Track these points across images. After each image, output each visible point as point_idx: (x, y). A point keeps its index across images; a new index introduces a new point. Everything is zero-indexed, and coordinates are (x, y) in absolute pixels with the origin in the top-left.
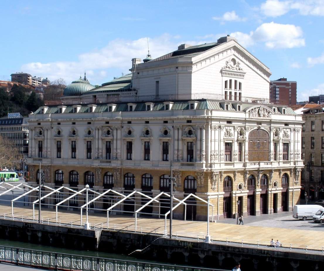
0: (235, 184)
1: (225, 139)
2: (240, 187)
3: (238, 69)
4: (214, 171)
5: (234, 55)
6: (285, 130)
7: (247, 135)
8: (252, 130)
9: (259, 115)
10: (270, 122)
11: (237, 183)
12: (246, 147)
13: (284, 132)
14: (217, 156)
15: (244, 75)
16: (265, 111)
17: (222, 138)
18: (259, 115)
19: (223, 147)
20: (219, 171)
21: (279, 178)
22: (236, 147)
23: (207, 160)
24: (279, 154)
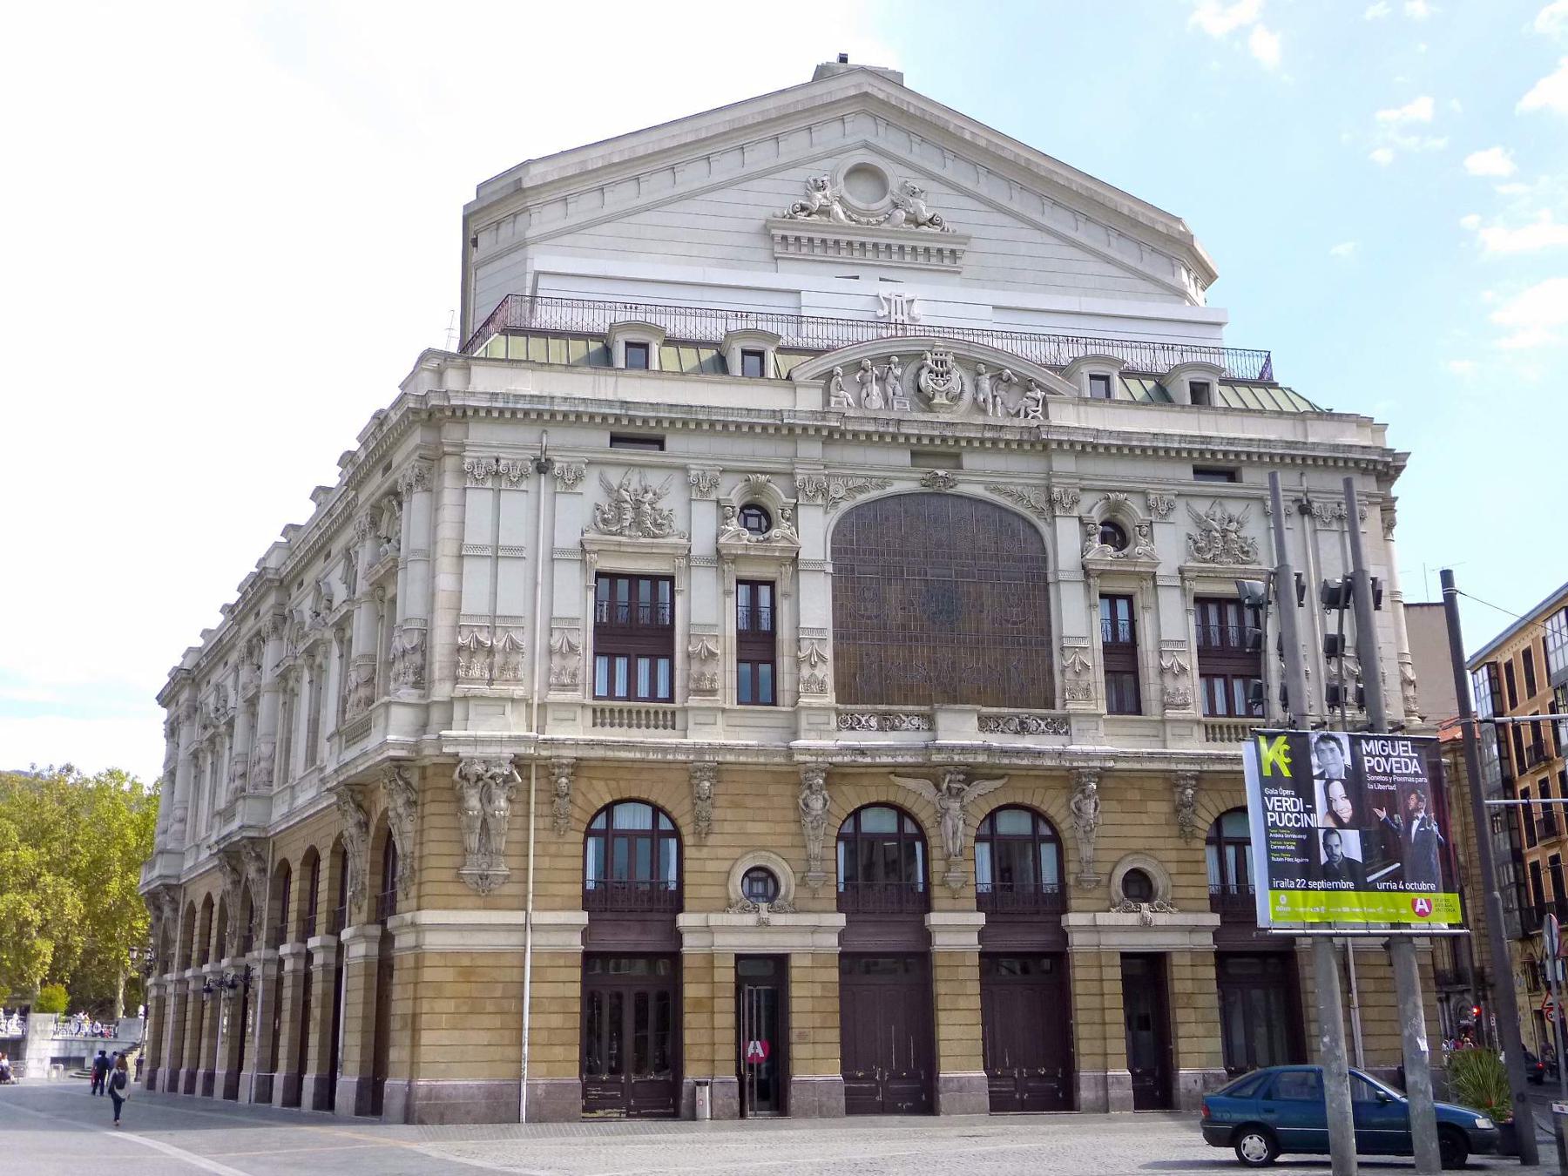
0: (711, 866)
1: (592, 542)
2: (762, 883)
3: (901, 215)
4: (464, 751)
5: (867, 146)
6: (1202, 507)
7: (813, 533)
8: (862, 498)
9: (924, 399)
10: (1038, 444)
11: (722, 852)
12: (812, 608)
13: (1198, 520)
14: (514, 659)
15: (953, 252)
16: (986, 384)
17: (568, 538)
18: (924, 399)
19: (576, 602)
20: (508, 752)
21: (1181, 843)
22: (706, 611)
23: (421, 679)
24: (1162, 671)
